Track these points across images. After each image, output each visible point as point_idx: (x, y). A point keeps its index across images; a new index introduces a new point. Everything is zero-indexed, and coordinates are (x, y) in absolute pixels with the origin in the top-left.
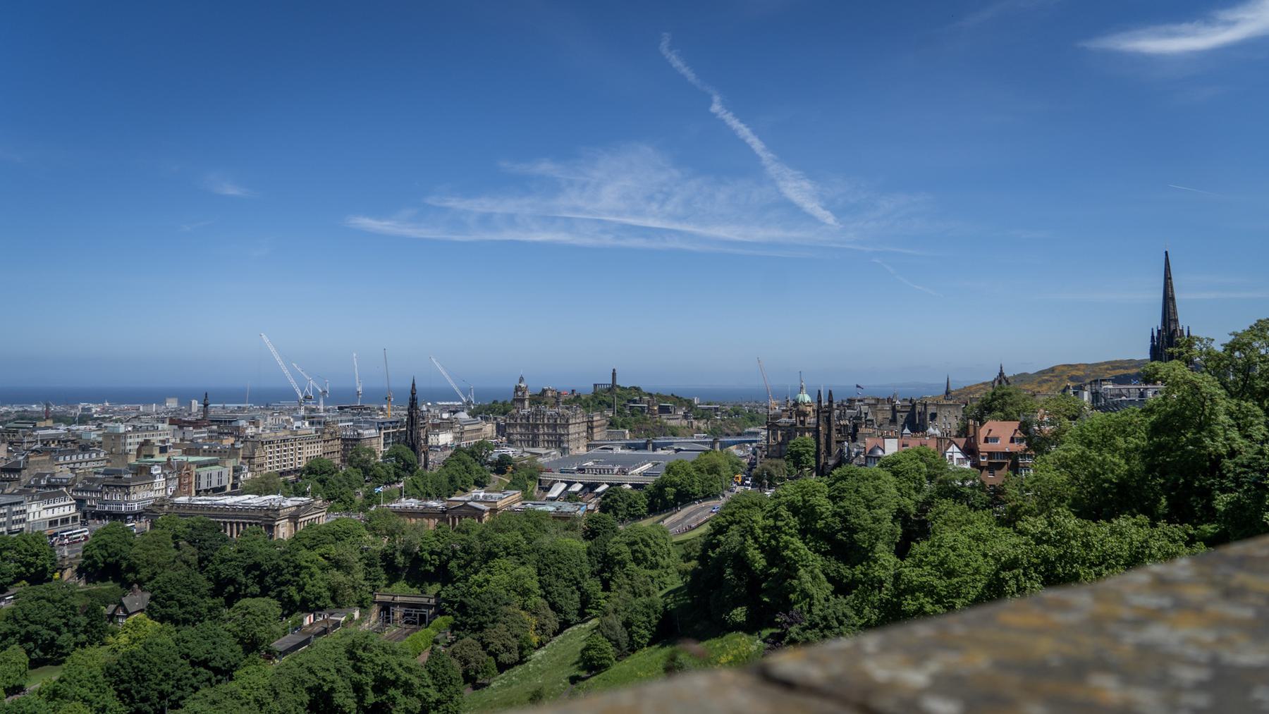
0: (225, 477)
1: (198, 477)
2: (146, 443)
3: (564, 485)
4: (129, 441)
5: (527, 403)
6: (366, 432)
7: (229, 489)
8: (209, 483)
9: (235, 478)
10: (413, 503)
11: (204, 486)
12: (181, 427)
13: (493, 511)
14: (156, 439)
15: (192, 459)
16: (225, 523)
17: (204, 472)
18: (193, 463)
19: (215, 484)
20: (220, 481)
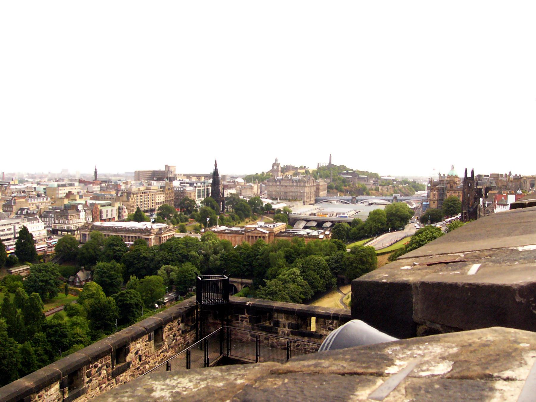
1: (101, 212)
2: (70, 192)
4: (60, 192)
5: (279, 173)
8: (107, 215)
9: (119, 213)
10: (223, 228)
11: (104, 217)
13: (271, 233)
14: (74, 191)
15: (98, 202)
16: (125, 237)
17: (104, 209)
18: (99, 204)
19: (110, 217)
20: (112, 215)
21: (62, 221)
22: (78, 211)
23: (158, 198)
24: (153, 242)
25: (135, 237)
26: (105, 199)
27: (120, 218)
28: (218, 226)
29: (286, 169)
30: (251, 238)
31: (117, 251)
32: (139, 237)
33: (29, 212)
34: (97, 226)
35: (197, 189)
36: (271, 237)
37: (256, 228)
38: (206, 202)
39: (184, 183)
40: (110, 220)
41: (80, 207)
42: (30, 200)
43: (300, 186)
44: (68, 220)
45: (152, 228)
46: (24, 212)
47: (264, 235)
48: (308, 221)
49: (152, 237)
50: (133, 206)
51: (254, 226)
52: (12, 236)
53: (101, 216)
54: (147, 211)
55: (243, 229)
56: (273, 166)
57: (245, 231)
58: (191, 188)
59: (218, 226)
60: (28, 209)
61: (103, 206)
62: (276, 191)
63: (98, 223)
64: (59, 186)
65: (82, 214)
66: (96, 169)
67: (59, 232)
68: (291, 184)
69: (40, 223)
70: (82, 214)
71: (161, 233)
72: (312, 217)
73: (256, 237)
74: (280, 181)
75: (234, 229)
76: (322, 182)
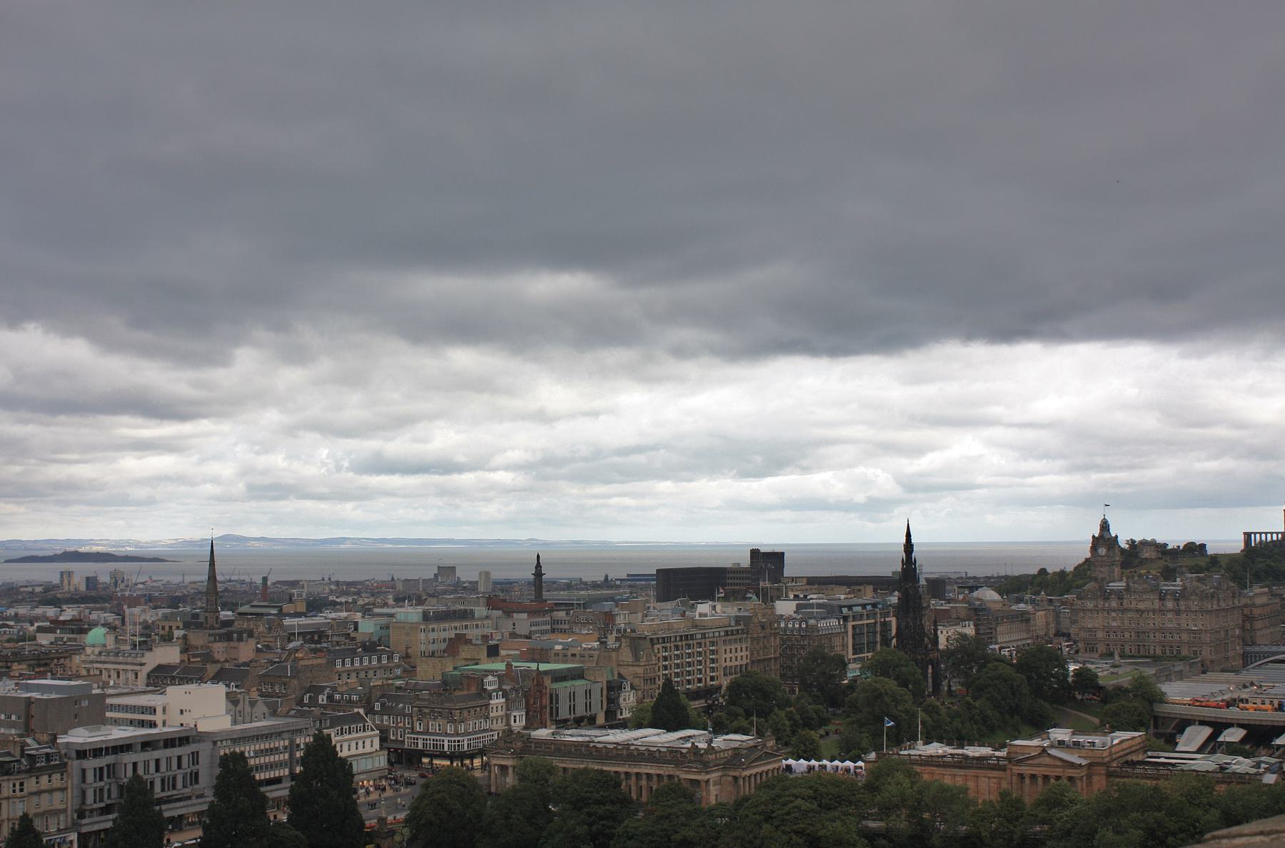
0: (596, 697)
1: (554, 698)
2: (460, 640)
3: (1207, 731)
6: (822, 624)
7: (601, 720)
8: (572, 709)
9: (610, 701)
10: (936, 749)
11: (564, 714)
12: (508, 614)
14: (473, 633)
15: (544, 667)
17: (563, 688)
18: (546, 673)
19: (580, 711)
20: (588, 706)
21: (434, 726)
22: (484, 694)
23: (728, 655)
24: (714, 791)
25: (659, 775)
26: (563, 657)
27: (612, 721)
28: (920, 742)
29: (1135, 555)
30: (1027, 781)
31: (601, 818)
32: (670, 777)
33: (337, 697)
34: (540, 743)
35: (850, 624)
36: (1095, 779)
37: (1044, 750)
38: (881, 668)
39: (812, 606)
40: (578, 722)
41: (491, 683)
42: (339, 661)
43: (1188, 611)
44: (454, 721)
45: (711, 749)
46: (322, 699)
47: (1072, 773)
48: (1219, 727)
49: (714, 776)
50: (653, 680)
51: (1035, 742)
52: (287, 772)
53: (554, 711)
54: (695, 695)
55: (1003, 753)
56: (1094, 548)
57: (1009, 758)
58: (834, 622)
59: (920, 742)
60: (334, 689)
61: (559, 677)
62: (1107, 629)
63: (543, 733)
64: (426, 617)
65: (498, 701)
66: (538, 566)
67: (425, 760)
68: (1157, 604)
69: (369, 733)
70: (498, 701)
71: (740, 766)
72: (1233, 713)
73: (1046, 778)
74: (1119, 595)
75: (973, 751)
76: (1258, 594)
